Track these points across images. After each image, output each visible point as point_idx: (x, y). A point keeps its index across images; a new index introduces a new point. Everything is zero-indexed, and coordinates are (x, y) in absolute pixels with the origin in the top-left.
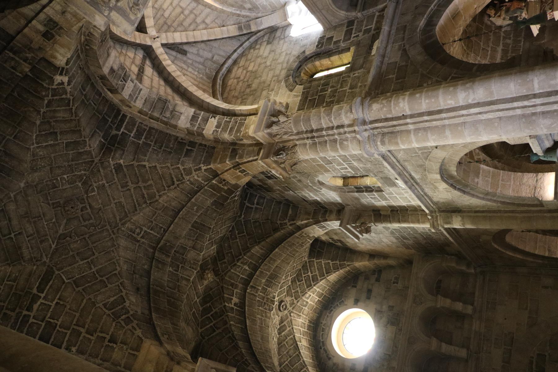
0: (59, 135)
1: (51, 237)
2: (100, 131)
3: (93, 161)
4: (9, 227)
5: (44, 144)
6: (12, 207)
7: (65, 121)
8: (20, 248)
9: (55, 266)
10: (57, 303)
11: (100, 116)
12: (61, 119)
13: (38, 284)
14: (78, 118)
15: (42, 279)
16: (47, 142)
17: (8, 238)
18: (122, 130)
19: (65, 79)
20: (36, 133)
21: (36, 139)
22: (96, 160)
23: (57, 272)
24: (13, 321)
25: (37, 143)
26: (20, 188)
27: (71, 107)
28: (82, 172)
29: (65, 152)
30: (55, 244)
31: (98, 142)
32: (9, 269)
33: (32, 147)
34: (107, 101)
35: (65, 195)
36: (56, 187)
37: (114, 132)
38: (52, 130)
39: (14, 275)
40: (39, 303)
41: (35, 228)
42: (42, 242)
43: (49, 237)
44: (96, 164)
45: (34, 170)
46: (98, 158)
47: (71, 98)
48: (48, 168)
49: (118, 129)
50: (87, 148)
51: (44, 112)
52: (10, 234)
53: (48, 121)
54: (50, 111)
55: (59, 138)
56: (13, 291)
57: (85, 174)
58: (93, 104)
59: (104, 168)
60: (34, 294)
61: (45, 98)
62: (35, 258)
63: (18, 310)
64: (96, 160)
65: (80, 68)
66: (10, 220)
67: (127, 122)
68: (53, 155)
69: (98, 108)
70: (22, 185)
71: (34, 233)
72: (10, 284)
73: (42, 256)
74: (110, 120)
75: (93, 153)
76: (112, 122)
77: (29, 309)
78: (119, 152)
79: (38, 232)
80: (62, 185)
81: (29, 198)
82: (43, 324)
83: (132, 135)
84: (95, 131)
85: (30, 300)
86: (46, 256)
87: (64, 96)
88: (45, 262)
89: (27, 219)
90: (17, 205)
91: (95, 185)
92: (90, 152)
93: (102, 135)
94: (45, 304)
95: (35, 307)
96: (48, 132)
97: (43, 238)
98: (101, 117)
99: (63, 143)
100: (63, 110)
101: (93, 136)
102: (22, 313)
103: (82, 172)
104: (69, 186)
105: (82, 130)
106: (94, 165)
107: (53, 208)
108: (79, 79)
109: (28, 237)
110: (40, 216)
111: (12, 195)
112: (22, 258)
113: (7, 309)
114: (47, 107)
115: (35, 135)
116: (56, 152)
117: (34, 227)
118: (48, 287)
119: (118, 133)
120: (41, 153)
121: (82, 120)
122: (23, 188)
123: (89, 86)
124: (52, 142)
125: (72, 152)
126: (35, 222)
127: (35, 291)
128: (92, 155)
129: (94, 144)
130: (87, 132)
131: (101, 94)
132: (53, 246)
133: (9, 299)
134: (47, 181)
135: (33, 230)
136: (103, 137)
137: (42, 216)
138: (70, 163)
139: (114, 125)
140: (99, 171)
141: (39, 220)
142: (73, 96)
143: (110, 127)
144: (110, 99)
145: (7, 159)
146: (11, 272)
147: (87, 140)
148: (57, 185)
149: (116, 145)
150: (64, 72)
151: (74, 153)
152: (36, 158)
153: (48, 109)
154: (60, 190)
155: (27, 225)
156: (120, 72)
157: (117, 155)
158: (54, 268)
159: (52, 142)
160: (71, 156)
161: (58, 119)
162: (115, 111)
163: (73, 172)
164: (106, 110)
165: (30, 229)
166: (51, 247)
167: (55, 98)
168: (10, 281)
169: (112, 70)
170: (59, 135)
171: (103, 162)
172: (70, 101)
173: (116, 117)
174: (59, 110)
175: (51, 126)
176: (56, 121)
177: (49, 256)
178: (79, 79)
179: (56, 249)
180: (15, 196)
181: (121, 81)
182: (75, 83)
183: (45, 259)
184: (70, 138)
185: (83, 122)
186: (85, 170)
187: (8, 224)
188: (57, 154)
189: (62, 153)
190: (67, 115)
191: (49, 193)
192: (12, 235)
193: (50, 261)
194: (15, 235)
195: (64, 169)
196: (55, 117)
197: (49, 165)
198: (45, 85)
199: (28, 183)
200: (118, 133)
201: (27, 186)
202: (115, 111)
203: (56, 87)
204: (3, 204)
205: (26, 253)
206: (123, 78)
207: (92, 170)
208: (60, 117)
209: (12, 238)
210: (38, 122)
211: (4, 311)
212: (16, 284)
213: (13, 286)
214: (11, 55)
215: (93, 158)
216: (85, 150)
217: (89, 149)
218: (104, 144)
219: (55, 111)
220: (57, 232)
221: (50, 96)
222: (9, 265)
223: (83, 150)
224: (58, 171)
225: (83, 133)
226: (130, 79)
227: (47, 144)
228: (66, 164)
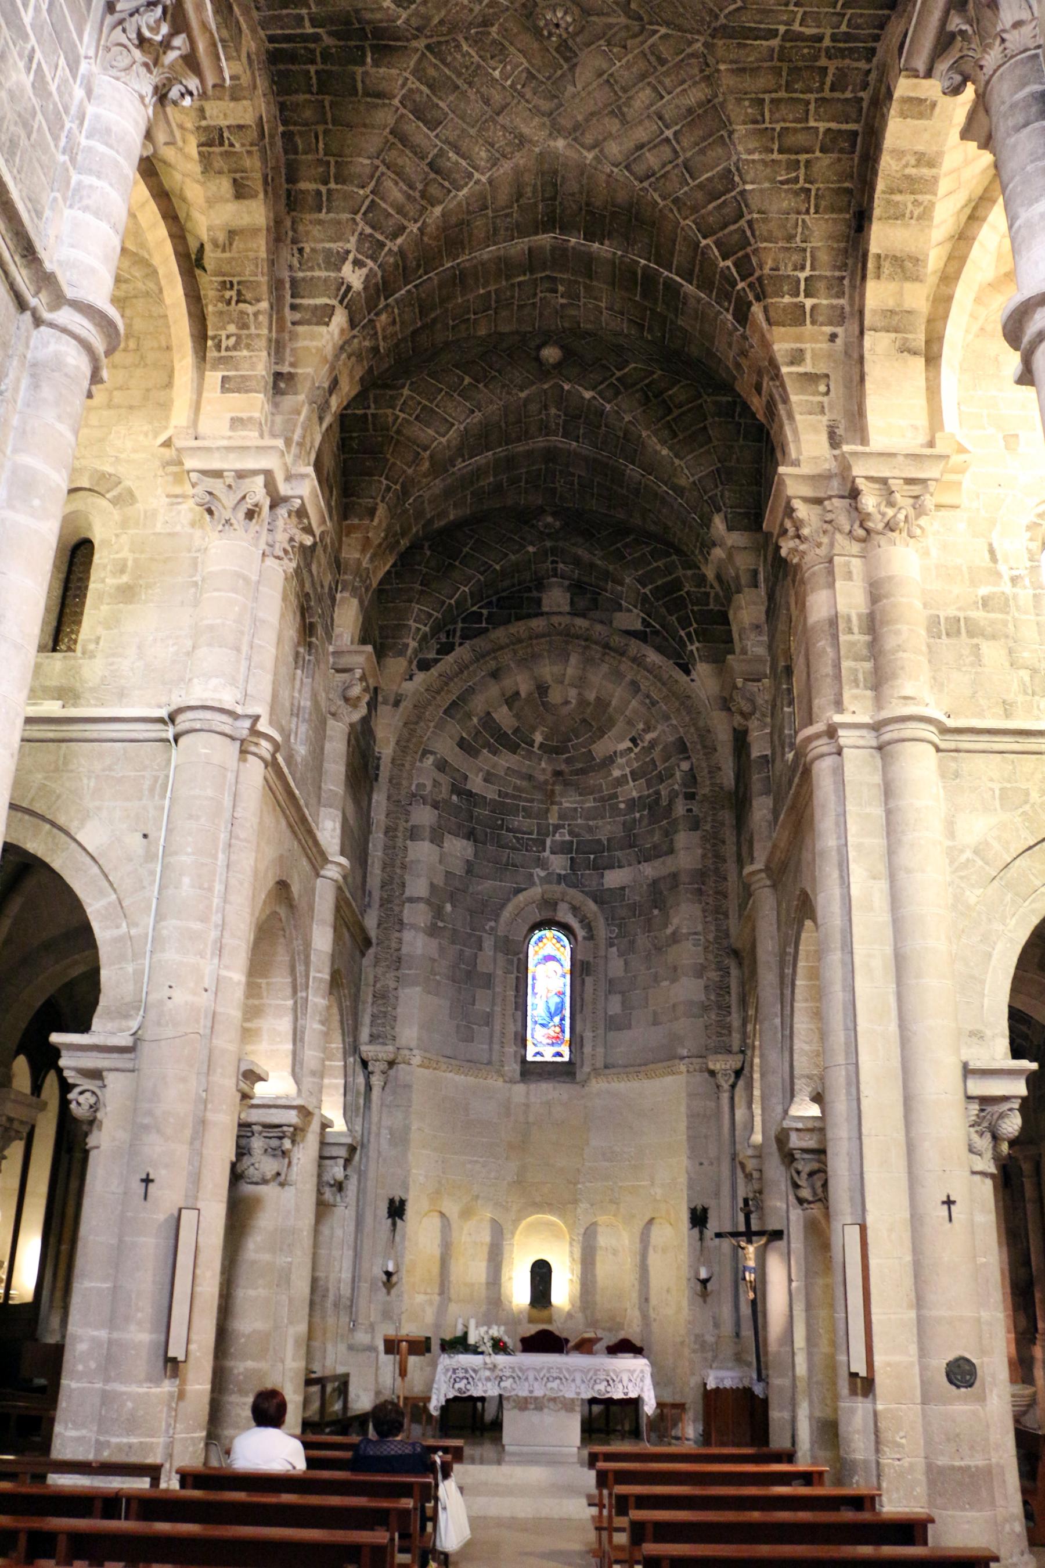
0: (430, 156)
1: (643, 43)
2: (354, 80)
3: (428, 47)
4: (655, 146)
5: (464, 163)
6: (614, 149)
7: (399, 173)
8: (690, 111)
9: (709, 23)
10: (796, 5)
11: (327, 104)
12: (401, 184)
13: (758, 42)
14: (377, 162)
15: (748, 38)
16: (457, 163)
17: (678, 143)
18: (311, 31)
19: (347, 269)
20: (456, 196)
21: (466, 184)
22: (420, 44)
23: (722, 20)
24: (847, 61)
25: (470, 176)
26: (569, 145)
27: (371, 197)
28: (465, 48)
29: (451, 115)
30: (656, 27)
31: (382, 70)
32: (741, 129)
33: (484, 179)
34: (282, 107)
35: (536, 45)
36: (529, 72)
37: (328, 41)
38: (432, 175)
39: (750, 110)
40: (802, 29)
41: (635, 85)
42: (662, 62)
43: (646, 46)
44: (432, 36)
45: (522, 141)
46: (415, 44)
47: (358, 218)
48: (500, 119)
49: (316, 38)
50: (413, 84)
51: (416, 221)
52: (667, 140)
53: (423, 197)
54: (405, 216)
55: (436, 151)
56: (782, 94)
57: (466, 39)
58: (321, 145)
59: (428, 19)
60: (783, 40)
61: (395, 249)
62: (702, 71)
63: (823, 62)
64: (420, 44)
65: (301, 251)
66: (640, 147)
67: (282, 28)
68: (472, 132)
69: (317, 123)
70: (560, 144)
71: (649, 84)
72: (770, 111)
73: (692, 55)
74: (312, 69)
75: (412, 64)
76: (313, 62)
77: (820, 38)
78: (368, 16)
79: (643, 76)
80: (517, 66)
81: (580, 118)
82: (850, 11)
83: (304, 11)
84: (367, 94)
85: (798, 43)
86: (690, 43)
87: (368, 230)
88: (706, 45)
89: (625, 109)
90: (605, 139)
91: (477, 8)
92: (419, 73)
93: (359, 70)
94: (802, 20)
95: (808, 31)
96: (439, 178)
97: (652, 59)
98: (327, 99)
99: (437, 136)
100: (385, 201)
101: (380, 95)
102: (828, 49)
103: (465, 48)
104: (512, 49)
105: (388, 130)
106: (434, 39)
107: (576, 55)
108: (316, 231)
109: (662, 97)
110: (608, 81)
111: (590, 156)
112: (709, 101)
113: (821, 89)
114: (405, 228)
115: (461, 194)
116: (463, 130)
117: (634, 90)
118: (762, 26)
119: (325, 37)
120: (483, 154)
121: (373, 150)
122: (565, 138)
123: (303, 185)
124: (451, 154)
125: (441, 104)
126: (625, 90)
127: (775, 43)
128: (420, 60)
129: (398, 77)
130: (385, 117)
131: (283, 134)
132: (663, 30)
133: (801, 96)
134: (527, 101)
135: (643, 89)
136: (363, 63)
137: (605, 77)
138: (466, 86)
139: (312, 51)
140: (442, 22)
141: (616, 82)
142: (354, 220)
143: (326, 56)
144: (271, 97)
145: (529, 189)
146: (744, 123)
147: (396, 102)
148: (524, 75)
149: (357, 26)
150: (343, 289)
151: (440, 98)
152: (497, 155)
153: (406, 223)
154: (529, 62)
155: (637, 104)
156: (219, 163)
157: (379, 16)
158: (713, 25)
159: (451, 154)
160: (451, 98)
161: (405, 188)
162: (282, 67)
163: (479, 66)
164: (302, 97)
165: (643, 96)
166: (665, 37)
167: (381, 238)
168: (763, 115)
169: (240, 191)
170: (430, 156)
171: (417, 29)
172: (364, 214)
173: (292, 57)
174: (392, 205)
175: (426, 185)
176: (411, 187)
177: (689, 36)
178: (317, 238)
179: (668, 24)
180: (590, 148)
181: (232, 145)
182: (332, 240)
183: (698, 46)
184: (419, 132)
185: (373, 142)
186: (458, 47)
187: (649, 150)
188: (465, 126)
189: (456, 120)
190: (388, 184)
191: (548, 78)
192: (669, 133)
193: (699, 32)
194: (668, 127)
195: (484, 89)
196: (409, 197)
197: (495, 122)
198: (380, 274)
199: (550, 135)
200: (325, 37)
201: (559, 132)
202: (282, 67)
203: (369, 262)
204: (615, 170)
205: (695, 95)
206: (222, 144)
207: (449, 32)
208: (401, 190)
209: (675, 133)
210: (438, 211)
211: (827, 94)
212: (767, 97)
213: (772, 101)
214: (382, 343)
215: (423, 54)
216: (418, 84)
217: (411, 77)
218: (375, 49)
219: (400, 210)
220: (627, 27)
221: (386, 249)
222: (731, 133)
223: (425, 89)
224: (497, 97)
225: (391, 121)
226: (204, 123)
227: (461, 161)
228: (471, 93)
